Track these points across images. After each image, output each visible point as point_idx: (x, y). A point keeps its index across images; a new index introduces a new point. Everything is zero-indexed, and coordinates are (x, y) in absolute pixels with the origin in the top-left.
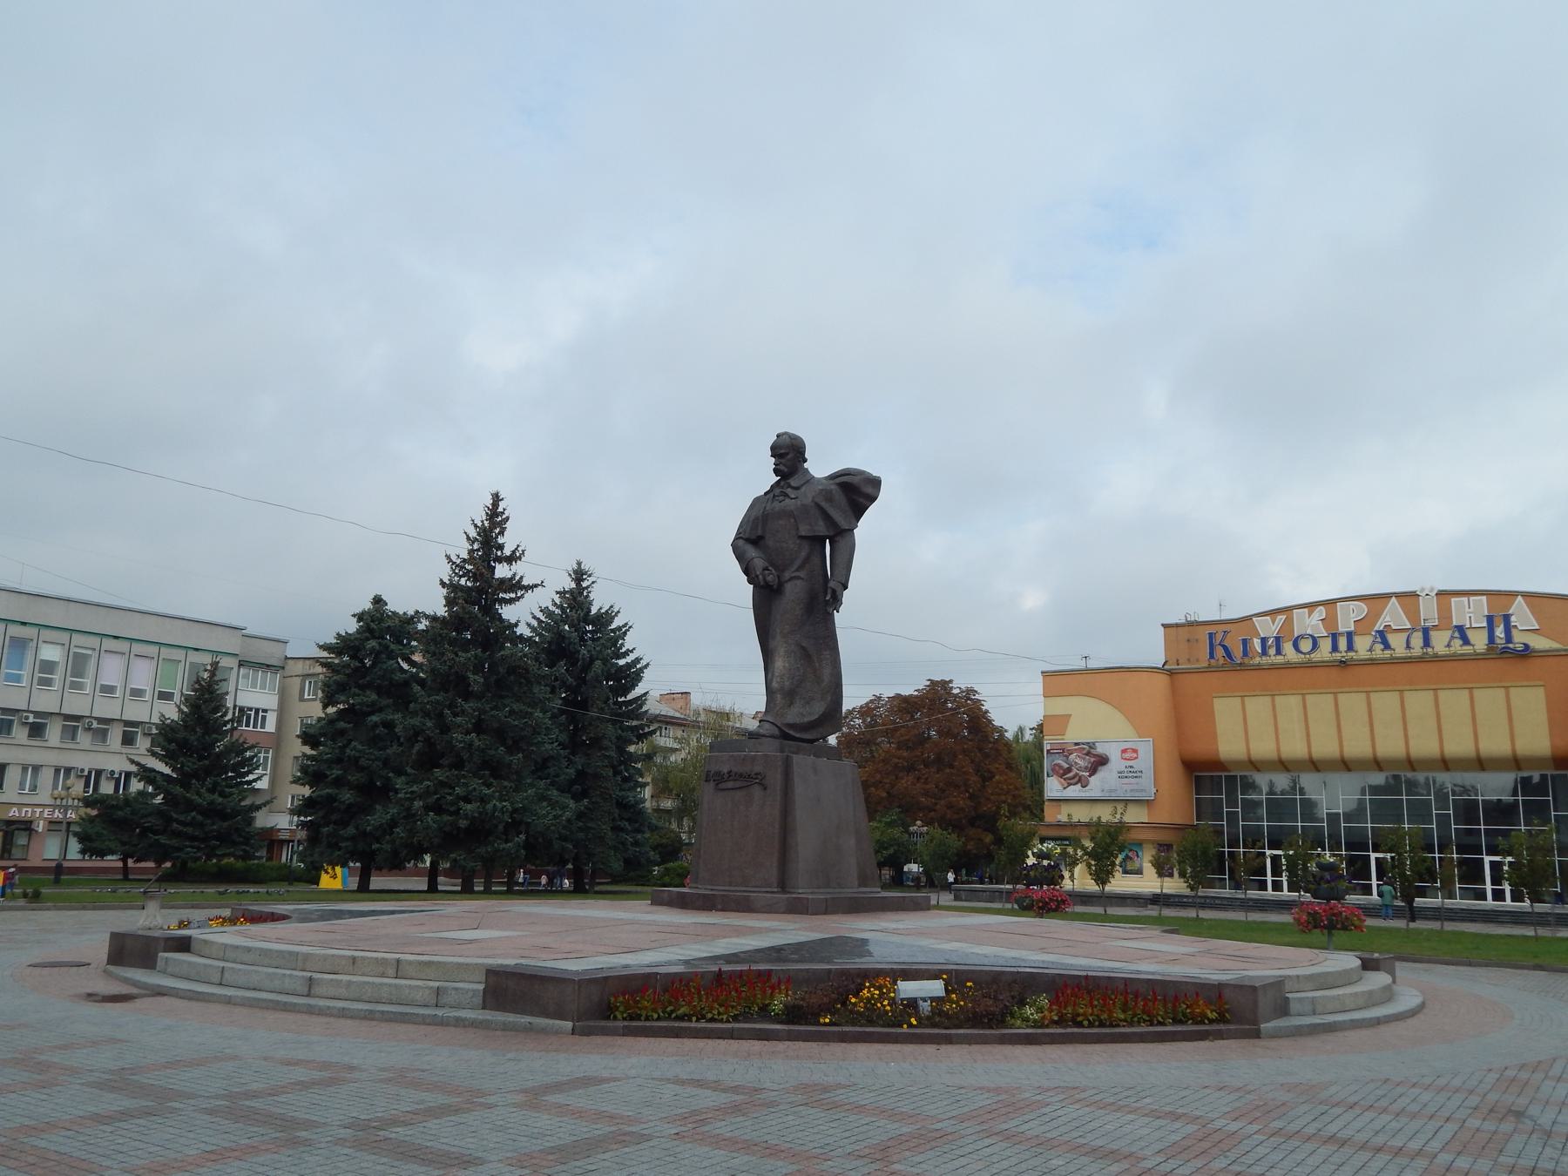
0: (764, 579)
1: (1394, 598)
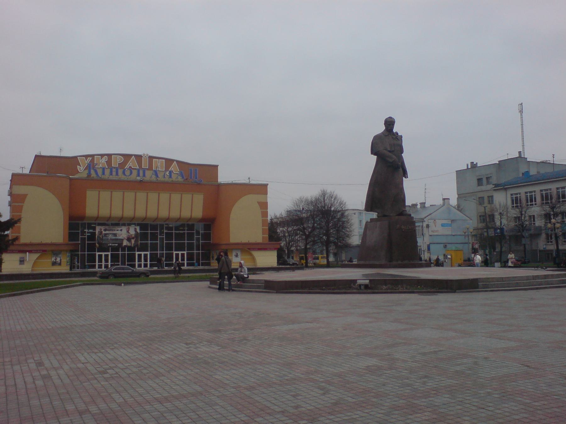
1: (133, 156)
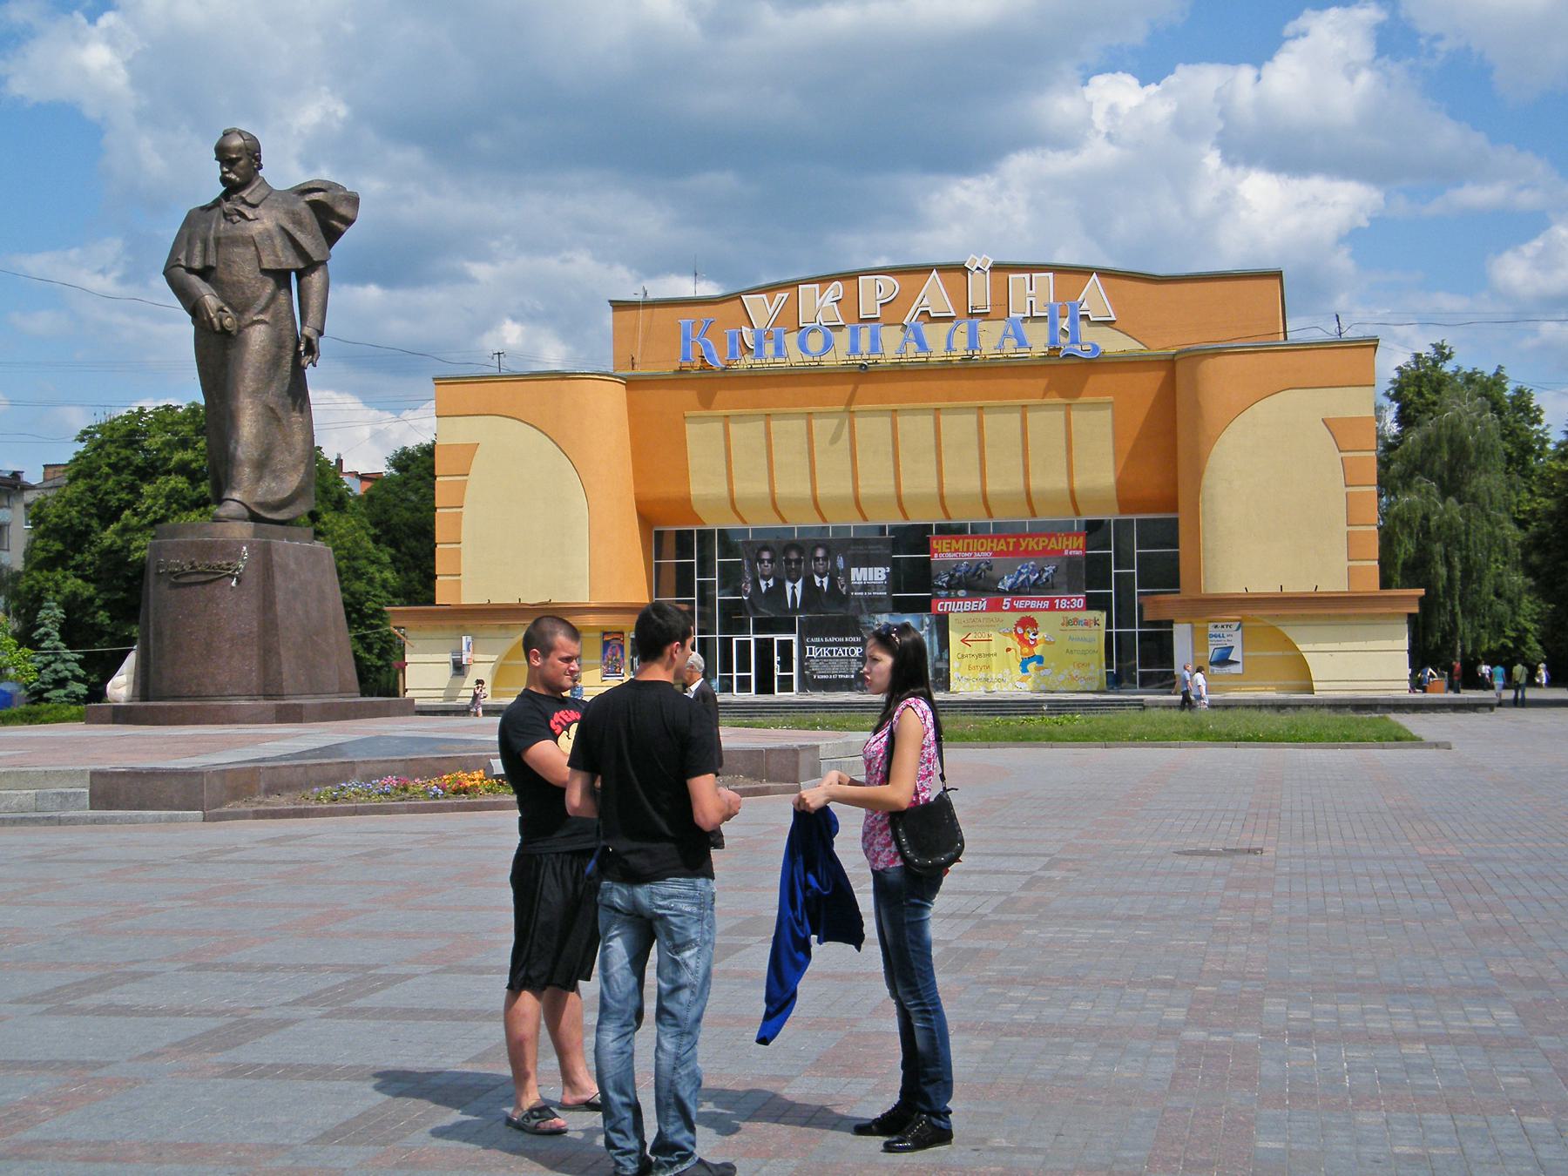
0: (221, 321)
